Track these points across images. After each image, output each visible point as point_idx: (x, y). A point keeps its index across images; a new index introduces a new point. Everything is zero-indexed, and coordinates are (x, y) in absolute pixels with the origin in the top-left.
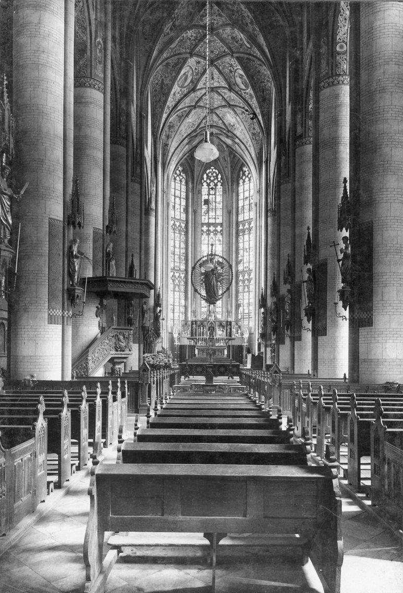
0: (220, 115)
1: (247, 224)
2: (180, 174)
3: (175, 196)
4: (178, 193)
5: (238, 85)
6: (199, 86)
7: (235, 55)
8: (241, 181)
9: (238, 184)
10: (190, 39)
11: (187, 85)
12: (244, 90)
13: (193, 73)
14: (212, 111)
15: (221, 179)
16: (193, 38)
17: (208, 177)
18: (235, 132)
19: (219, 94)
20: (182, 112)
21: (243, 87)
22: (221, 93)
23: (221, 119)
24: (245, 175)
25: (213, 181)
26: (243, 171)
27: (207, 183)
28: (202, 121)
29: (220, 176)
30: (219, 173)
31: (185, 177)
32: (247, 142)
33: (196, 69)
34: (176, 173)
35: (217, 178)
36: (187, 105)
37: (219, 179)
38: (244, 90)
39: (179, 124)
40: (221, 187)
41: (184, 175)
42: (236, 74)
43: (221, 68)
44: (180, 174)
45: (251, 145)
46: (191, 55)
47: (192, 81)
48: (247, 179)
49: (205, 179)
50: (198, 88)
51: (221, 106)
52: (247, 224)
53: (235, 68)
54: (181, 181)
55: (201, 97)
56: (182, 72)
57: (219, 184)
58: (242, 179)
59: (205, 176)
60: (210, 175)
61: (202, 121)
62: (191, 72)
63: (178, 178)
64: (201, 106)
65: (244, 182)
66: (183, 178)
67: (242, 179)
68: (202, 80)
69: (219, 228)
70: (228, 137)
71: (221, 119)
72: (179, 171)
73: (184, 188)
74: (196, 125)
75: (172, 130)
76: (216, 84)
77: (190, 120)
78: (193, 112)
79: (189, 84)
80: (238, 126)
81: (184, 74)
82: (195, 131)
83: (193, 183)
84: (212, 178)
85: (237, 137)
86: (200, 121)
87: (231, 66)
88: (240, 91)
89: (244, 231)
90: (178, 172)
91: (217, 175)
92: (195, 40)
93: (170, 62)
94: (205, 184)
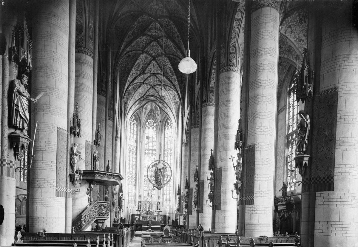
0: (157, 90)
1: (169, 151)
2: (133, 121)
3: (130, 133)
4: (132, 131)
5: (168, 74)
6: (146, 71)
7: (168, 56)
8: (166, 128)
9: (165, 129)
10: (142, 42)
11: (140, 70)
12: (171, 76)
13: (143, 63)
14: (153, 87)
15: (156, 125)
16: (144, 42)
17: (149, 123)
18: (165, 100)
19: (157, 78)
20: (136, 86)
21: (171, 75)
22: (158, 77)
23: (157, 92)
24: (169, 125)
25: (151, 126)
26: (167, 122)
27: (148, 127)
28: (146, 92)
29: (155, 124)
30: (155, 122)
31: (136, 123)
32: (171, 106)
33: (145, 61)
34: (131, 120)
35: (154, 125)
36: (139, 81)
37: (155, 126)
38: (171, 76)
39: (134, 92)
40: (156, 130)
41: (136, 122)
42: (167, 67)
43: (159, 62)
44: (133, 121)
45: (173, 107)
46: (143, 53)
47: (142, 68)
48: (170, 127)
49: (147, 125)
50: (146, 72)
51: (157, 85)
52: (169, 151)
53: (167, 64)
54: (134, 124)
55: (147, 78)
56: (137, 62)
57: (155, 128)
58: (167, 126)
59: (147, 123)
60: (150, 123)
61: (146, 92)
62: (142, 63)
63: (132, 123)
64: (147, 83)
65: (168, 128)
66: (135, 123)
67: (167, 126)
68: (148, 68)
69: (154, 152)
70: (160, 102)
71: (157, 92)
72: (133, 119)
73: (135, 129)
74: (143, 94)
75: (130, 95)
76: (156, 72)
77: (140, 91)
78: (142, 86)
79: (141, 69)
80: (166, 97)
81: (138, 63)
82: (143, 97)
83: (140, 126)
84: (151, 125)
85: (166, 103)
86: (145, 92)
87: (165, 62)
88: (169, 77)
89: (167, 154)
90: (132, 119)
91: (154, 123)
92: (145, 43)
93: (130, 54)
94: (147, 127)
